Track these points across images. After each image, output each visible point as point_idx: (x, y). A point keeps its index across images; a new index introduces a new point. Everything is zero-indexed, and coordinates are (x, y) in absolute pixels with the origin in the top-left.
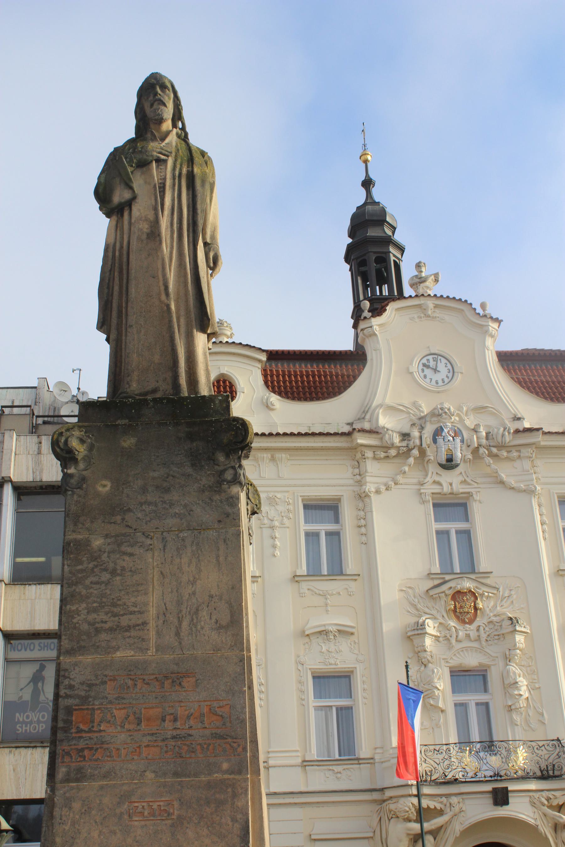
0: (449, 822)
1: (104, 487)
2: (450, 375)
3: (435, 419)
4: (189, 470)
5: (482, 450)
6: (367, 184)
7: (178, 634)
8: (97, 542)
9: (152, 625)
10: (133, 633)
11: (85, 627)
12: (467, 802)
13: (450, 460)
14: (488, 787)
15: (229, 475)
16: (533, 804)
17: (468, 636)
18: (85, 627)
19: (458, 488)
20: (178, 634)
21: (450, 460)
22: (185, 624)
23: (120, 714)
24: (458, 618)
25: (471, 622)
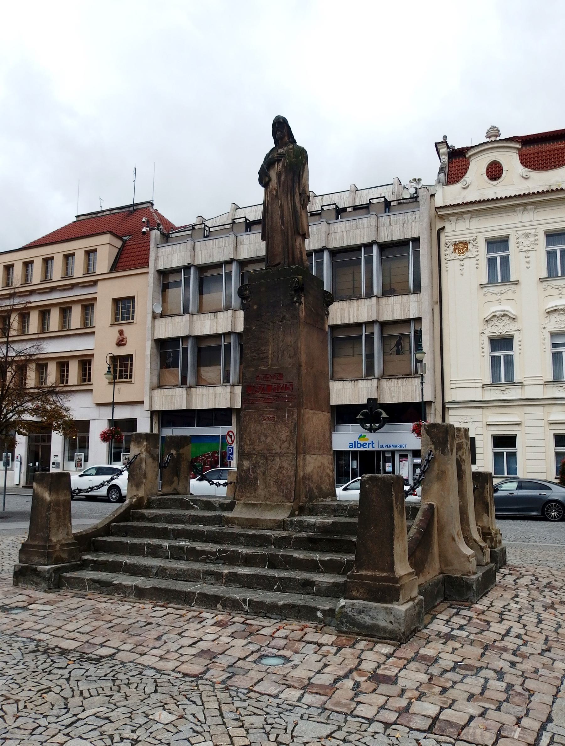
7: (277, 360)
9: (270, 356)
11: (250, 358)
18: (250, 358)
20: (277, 360)
22: (280, 356)
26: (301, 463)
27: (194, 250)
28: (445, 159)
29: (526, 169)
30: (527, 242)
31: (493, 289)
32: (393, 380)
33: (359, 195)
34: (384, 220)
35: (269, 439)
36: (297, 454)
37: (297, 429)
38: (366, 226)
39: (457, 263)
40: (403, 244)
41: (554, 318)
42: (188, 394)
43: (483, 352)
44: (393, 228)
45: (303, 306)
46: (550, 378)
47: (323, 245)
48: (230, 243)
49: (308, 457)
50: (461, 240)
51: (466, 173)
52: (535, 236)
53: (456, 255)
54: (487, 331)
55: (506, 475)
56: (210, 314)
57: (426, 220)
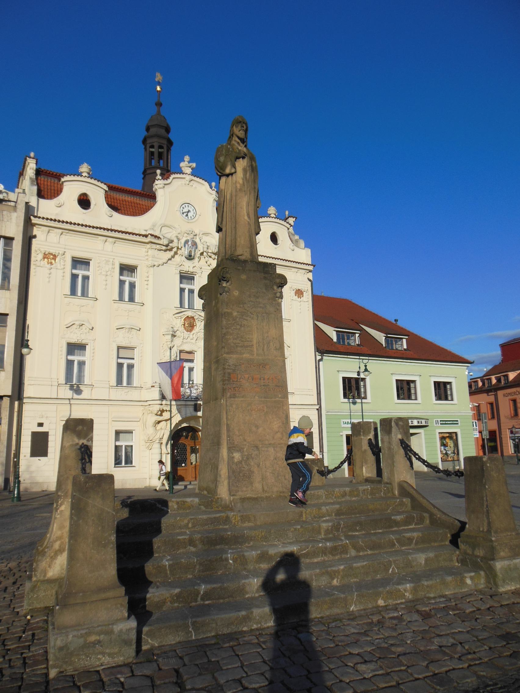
1: (236, 293)
2: (195, 215)
4: (264, 291)
5: (205, 254)
7: (263, 350)
8: (235, 314)
9: (255, 346)
10: (249, 349)
11: (232, 345)
15: (278, 295)
18: (232, 345)
19: (191, 270)
20: (263, 350)
21: (190, 256)
22: (265, 347)
23: (247, 376)
25: (191, 331)
35: (260, 430)
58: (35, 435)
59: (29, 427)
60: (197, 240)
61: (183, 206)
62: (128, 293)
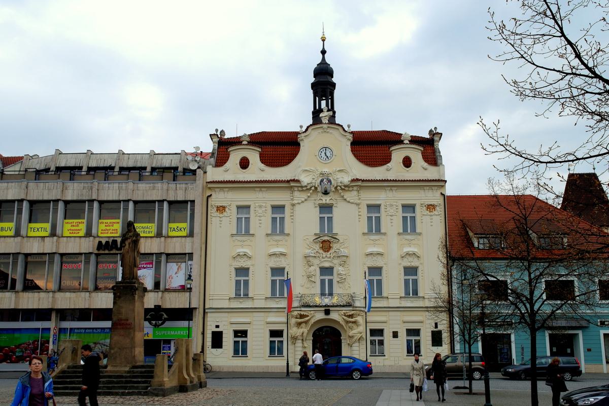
0: (310, 319)
2: (331, 156)
3: (321, 175)
5: (338, 188)
6: (324, 52)
12: (317, 313)
13: (326, 191)
14: (323, 309)
16: (339, 315)
17: (326, 256)
19: (328, 202)
21: (326, 191)
24: (323, 250)
25: (328, 251)
26: (133, 351)
27: (27, 188)
28: (217, 145)
29: (263, 165)
30: (260, 211)
31: (239, 238)
32: (172, 293)
33: (156, 158)
34: (172, 185)
36: (131, 348)
37: (133, 339)
38: (160, 188)
39: (218, 219)
40: (186, 202)
41: (273, 259)
42: (16, 297)
43: (231, 277)
44: (178, 192)
45: (136, 296)
46: (269, 295)
47: (129, 198)
48: (58, 187)
49: (136, 349)
50: (221, 205)
51: (225, 163)
52: (266, 207)
53: (218, 214)
54: (233, 264)
55: (240, 355)
56: (38, 238)
57: (201, 190)
58: (213, 333)
59: (210, 329)
60: (331, 178)
61: (322, 150)
62: (278, 227)
